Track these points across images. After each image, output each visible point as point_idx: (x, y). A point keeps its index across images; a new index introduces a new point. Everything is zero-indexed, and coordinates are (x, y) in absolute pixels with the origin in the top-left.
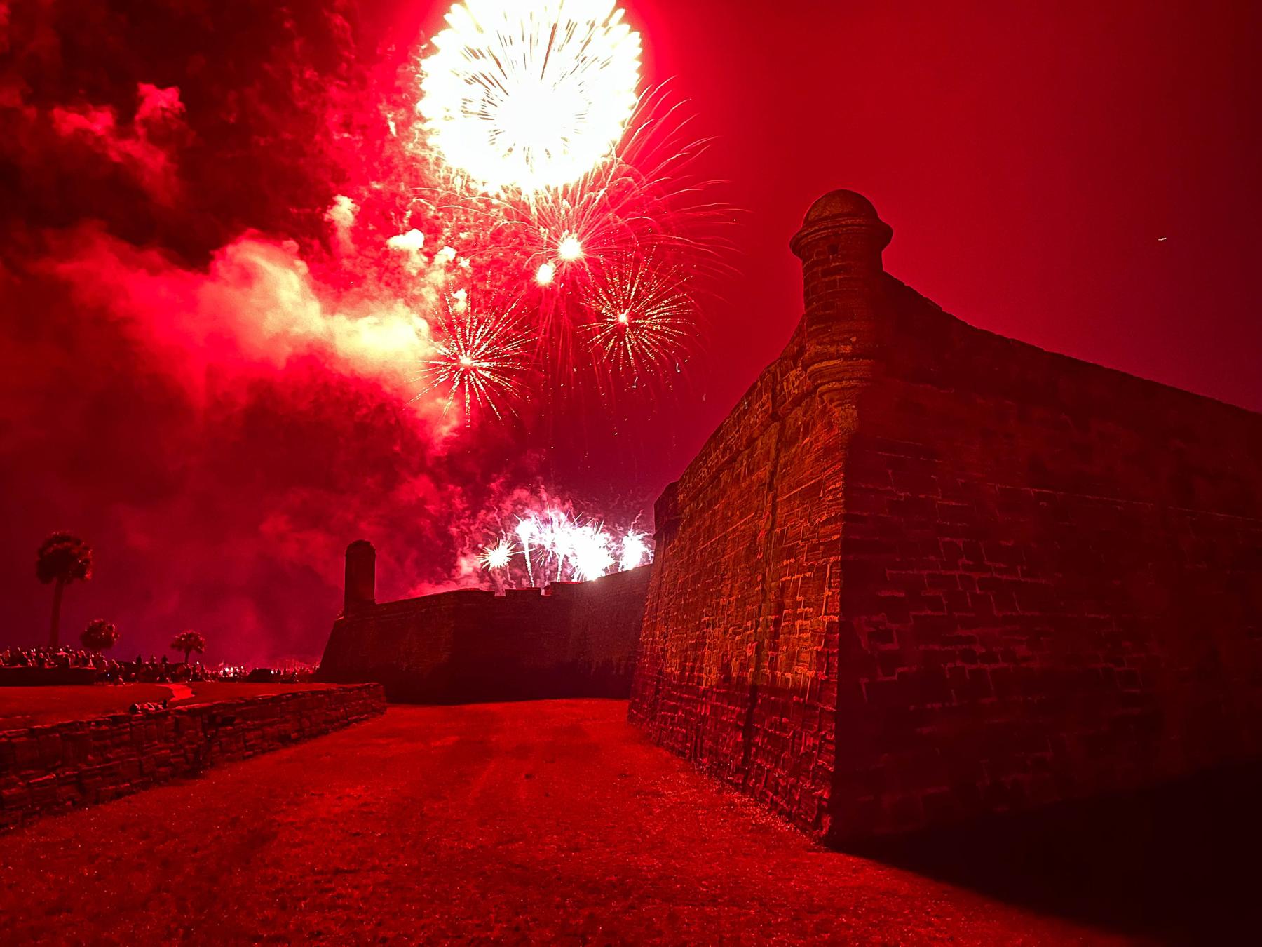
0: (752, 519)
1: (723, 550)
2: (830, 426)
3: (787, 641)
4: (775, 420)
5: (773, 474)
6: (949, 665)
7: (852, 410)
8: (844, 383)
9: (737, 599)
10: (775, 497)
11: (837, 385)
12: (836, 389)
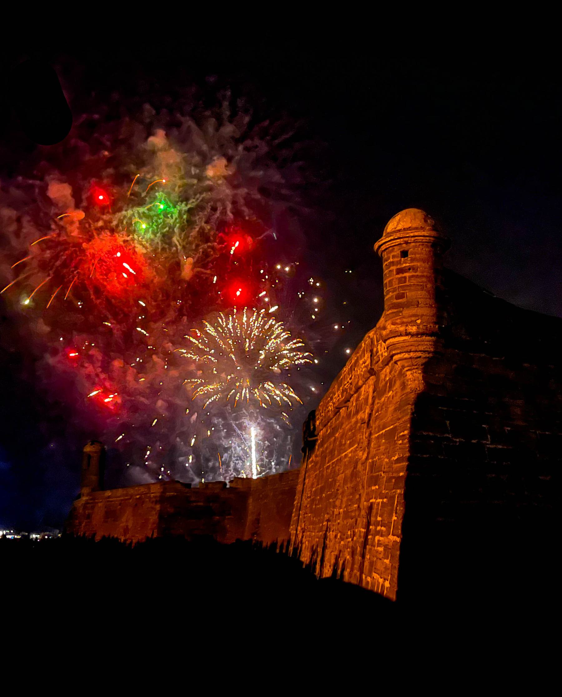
0: (356, 450)
1: (339, 470)
2: (404, 386)
4: (372, 375)
5: (370, 415)
8: (412, 354)
10: (371, 434)
11: (407, 356)
12: (406, 359)
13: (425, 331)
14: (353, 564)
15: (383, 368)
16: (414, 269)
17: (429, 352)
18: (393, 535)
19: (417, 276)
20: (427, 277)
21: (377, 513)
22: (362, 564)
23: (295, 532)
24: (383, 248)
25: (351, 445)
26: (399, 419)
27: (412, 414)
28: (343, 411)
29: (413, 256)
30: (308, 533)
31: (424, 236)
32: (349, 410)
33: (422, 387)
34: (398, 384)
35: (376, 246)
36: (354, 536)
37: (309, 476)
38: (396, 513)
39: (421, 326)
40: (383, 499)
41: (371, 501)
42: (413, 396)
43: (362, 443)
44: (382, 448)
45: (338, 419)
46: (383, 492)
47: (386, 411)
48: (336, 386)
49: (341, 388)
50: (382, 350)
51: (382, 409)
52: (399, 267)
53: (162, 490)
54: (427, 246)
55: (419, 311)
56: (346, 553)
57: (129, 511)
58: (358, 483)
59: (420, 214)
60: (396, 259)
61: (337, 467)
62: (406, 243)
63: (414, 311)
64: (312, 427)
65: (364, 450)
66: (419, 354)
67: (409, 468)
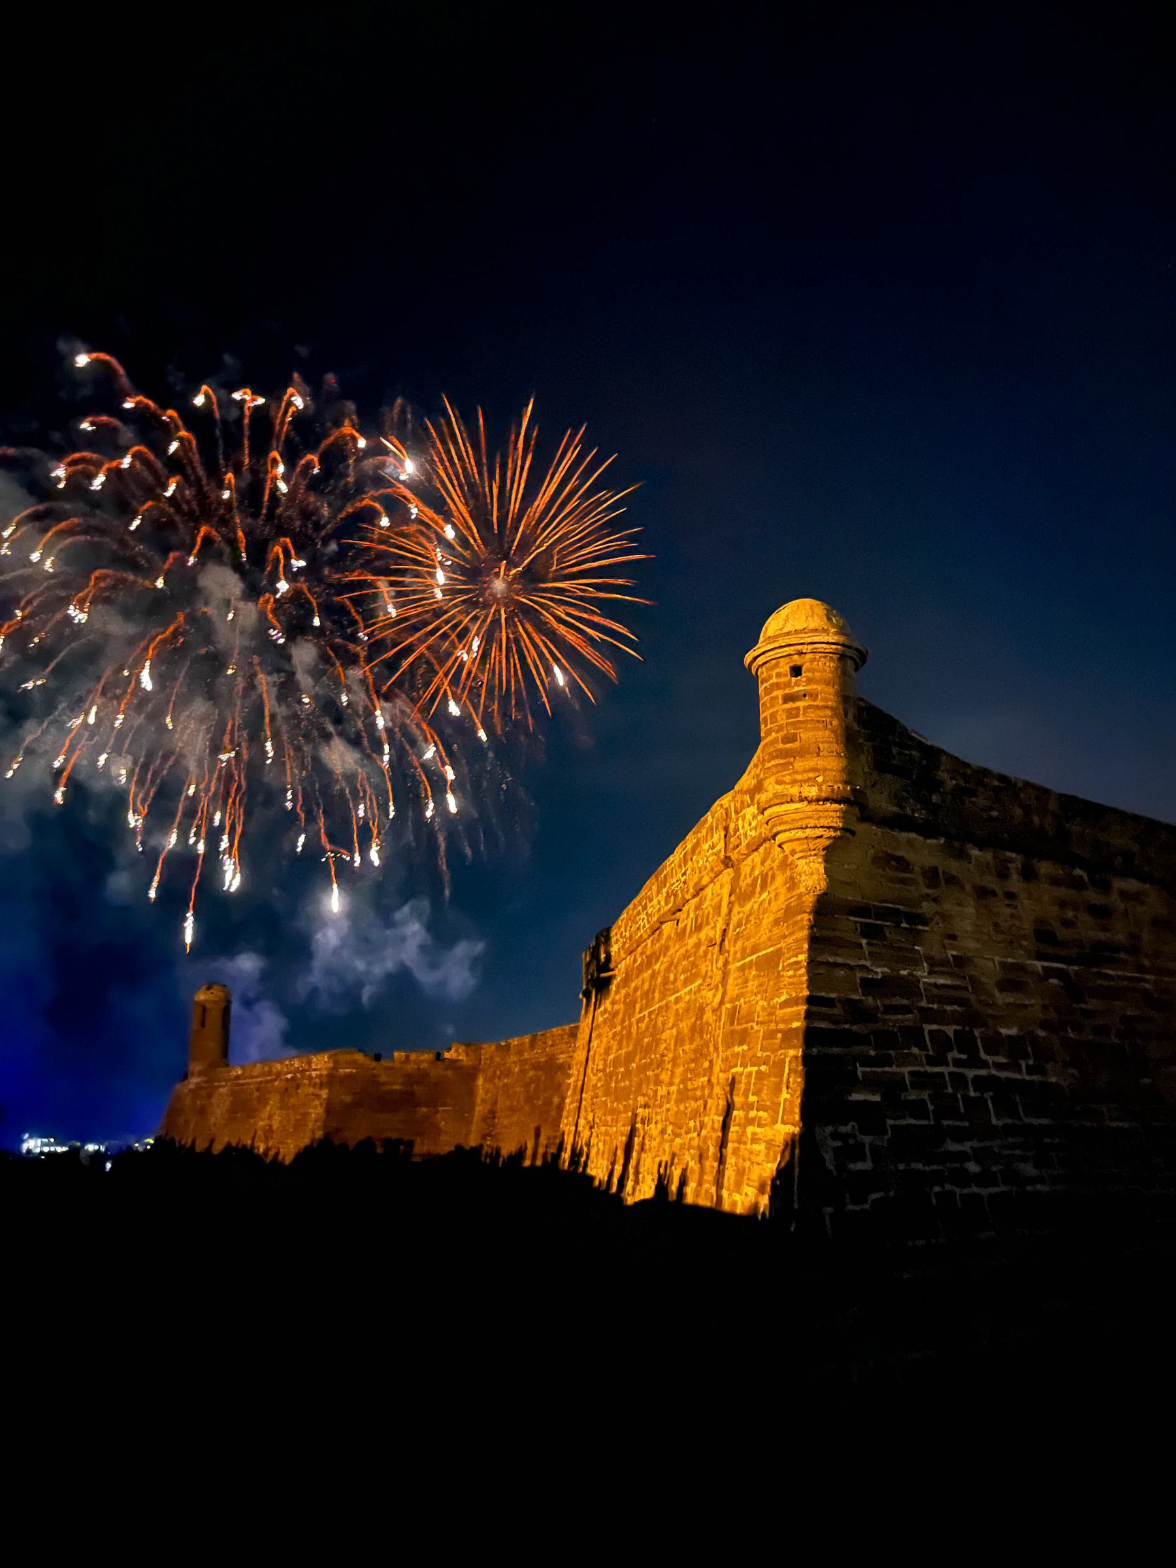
0: (699, 990)
2: (792, 883)
3: (736, 1151)
6: (937, 1189)
7: (818, 865)
9: (679, 1091)
10: (726, 963)
11: (800, 834)
12: (799, 839)
13: (831, 795)
14: (702, 1172)
15: (748, 855)
16: (813, 696)
17: (835, 829)
18: (783, 1123)
19: (818, 707)
20: (831, 708)
21: (747, 1091)
22: (720, 1173)
23: (573, 1128)
24: (760, 661)
25: (686, 982)
26: (785, 937)
27: (811, 927)
28: (667, 928)
29: (810, 675)
30: (603, 1129)
31: (828, 643)
32: (681, 925)
33: (823, 884)
34: (779, 880)
35: (748, 658)
36: (701, 1128)
37: (599, 1036)
38: (788, 1088)
39: (824, 787)
40: (759, 1065)
41: (734, 1070)
42: (809, 900)
43: (711, 977)
44: (752, 985)
45: (658, 941)
46: (759, 1054)
47: (758, 925)
48: (654, 888)
49: (664, 890)
50: (749, 823)
51: (748, 921)
52: (787, 691)
53: (331, 1065)
54: (832, 659)
55: (819, 763)
56: (687, 1157)
57: (273, 1101)
58: (706, 1044)
59: (822, 607)
60: (782, 680)
61: (660, 1019)
62: (801, 653)
63: (812, 762)
64: (603, 956)
65: (717, 988)
66: (819, 832)
67: (808, 1015)
